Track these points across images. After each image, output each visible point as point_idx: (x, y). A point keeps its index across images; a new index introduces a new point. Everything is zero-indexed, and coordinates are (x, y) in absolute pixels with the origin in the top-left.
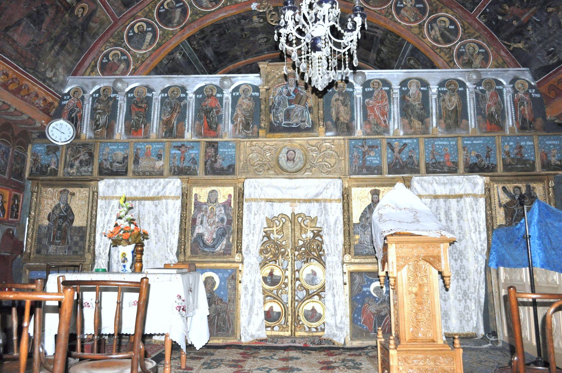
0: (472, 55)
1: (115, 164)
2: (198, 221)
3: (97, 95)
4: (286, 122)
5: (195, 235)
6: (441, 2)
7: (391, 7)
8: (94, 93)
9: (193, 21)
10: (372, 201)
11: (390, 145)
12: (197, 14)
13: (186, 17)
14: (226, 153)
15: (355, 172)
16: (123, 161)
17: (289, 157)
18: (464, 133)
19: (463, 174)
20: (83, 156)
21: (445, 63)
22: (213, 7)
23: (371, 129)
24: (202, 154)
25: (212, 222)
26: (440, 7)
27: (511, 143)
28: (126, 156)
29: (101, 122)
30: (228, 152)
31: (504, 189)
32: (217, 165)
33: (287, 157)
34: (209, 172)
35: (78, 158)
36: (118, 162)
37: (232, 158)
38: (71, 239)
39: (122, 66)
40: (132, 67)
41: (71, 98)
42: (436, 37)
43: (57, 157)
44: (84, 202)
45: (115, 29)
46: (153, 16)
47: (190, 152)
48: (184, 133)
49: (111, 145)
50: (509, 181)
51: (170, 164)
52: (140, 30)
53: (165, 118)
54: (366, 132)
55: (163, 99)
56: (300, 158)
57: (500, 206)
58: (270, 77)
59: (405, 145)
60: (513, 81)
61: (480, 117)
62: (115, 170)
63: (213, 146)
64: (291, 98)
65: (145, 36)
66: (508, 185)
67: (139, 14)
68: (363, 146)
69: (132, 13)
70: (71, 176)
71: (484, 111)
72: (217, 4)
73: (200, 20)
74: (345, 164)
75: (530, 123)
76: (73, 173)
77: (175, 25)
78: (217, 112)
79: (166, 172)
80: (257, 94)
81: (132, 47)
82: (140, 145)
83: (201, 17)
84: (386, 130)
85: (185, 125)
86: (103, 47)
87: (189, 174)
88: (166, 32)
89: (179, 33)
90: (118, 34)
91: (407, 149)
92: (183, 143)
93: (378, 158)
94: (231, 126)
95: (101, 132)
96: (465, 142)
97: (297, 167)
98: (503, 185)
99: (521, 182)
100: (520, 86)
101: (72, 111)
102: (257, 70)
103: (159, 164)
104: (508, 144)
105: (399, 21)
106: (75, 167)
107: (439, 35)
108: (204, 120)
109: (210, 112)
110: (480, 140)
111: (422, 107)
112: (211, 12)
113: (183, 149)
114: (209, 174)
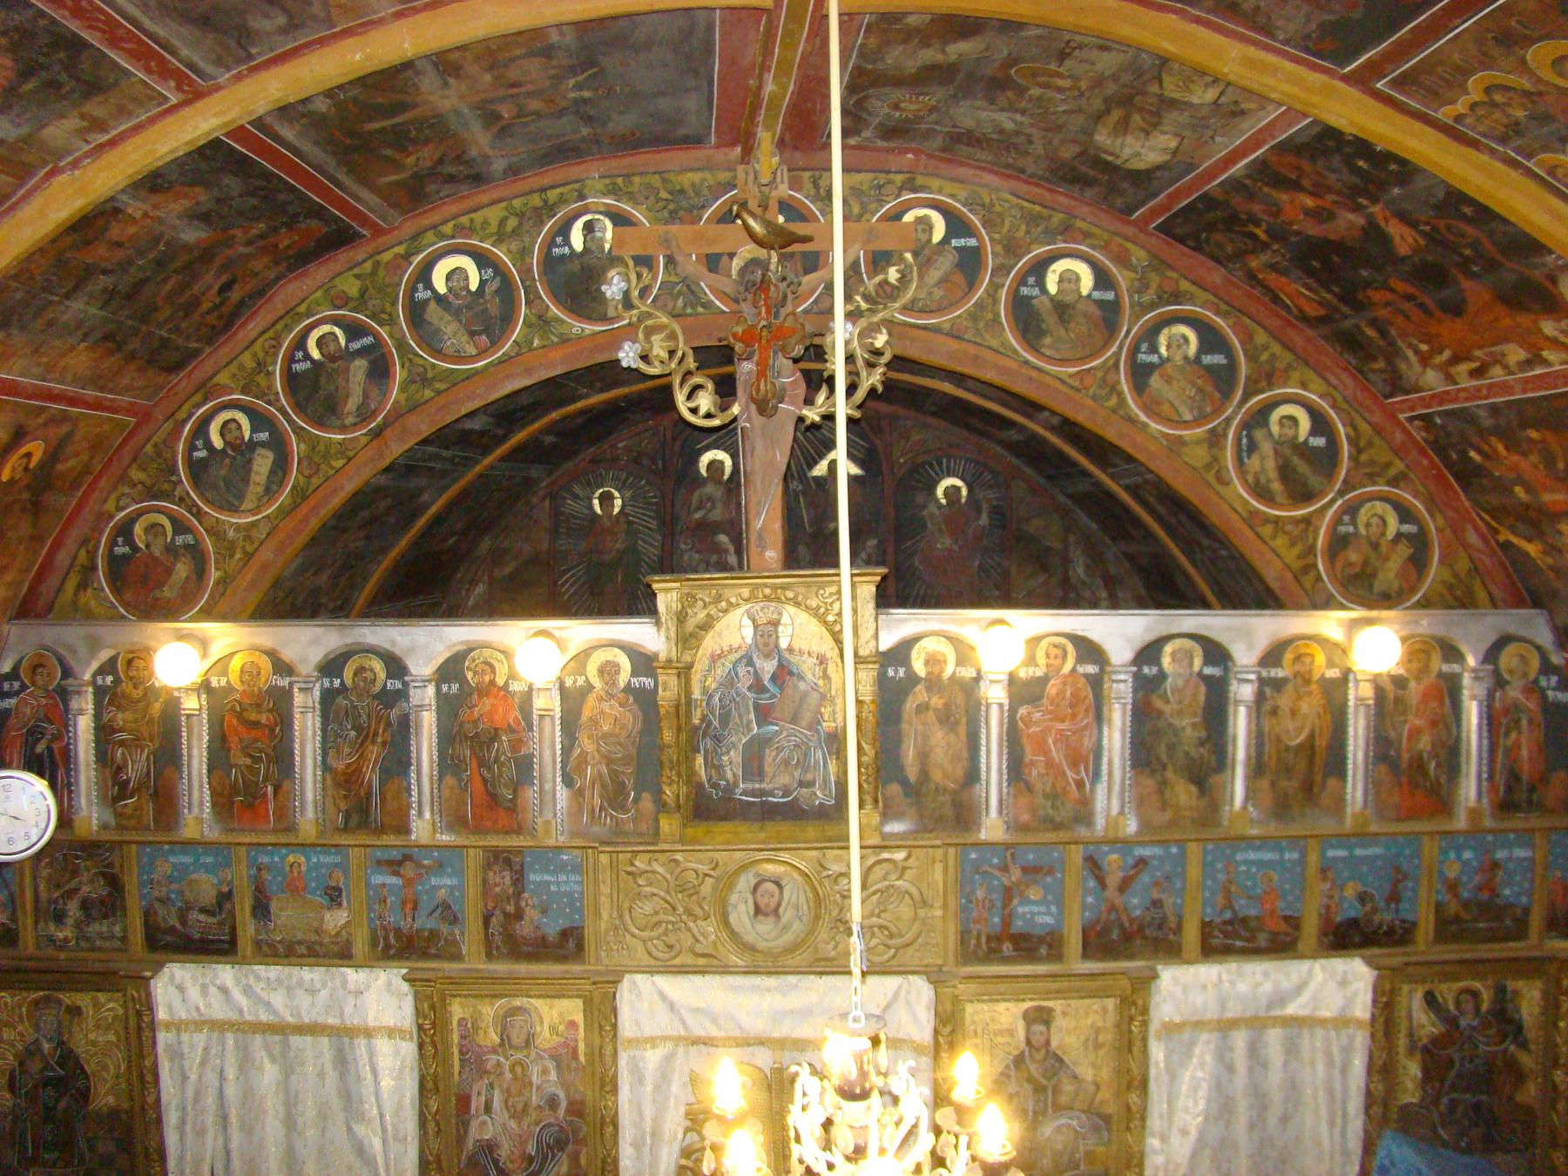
0: (1375, 546)
1: (194, 916)
2: (477, 1102)
3: (109, 679)
5: (470, 1144)
7: (1116, 365)
8: (94, 675)
9: (414, 407)
10: (1028, 1042)
11: (1093, 865)
12: (425, 381)
13: (385, 393)
15: (975, 952)
16: (220, 906)
17: (762, 902)
18: (1327, 825)
19: (1314, 957)
20: (92, 888)
21: (1289, 576)
22: (482, 353)
24: (473, 891)
25: (520, 1107)
26: (1280, 365)
27: (1467, 855)
28: (225, 889)
30: (558, 883)
31: (1430, 999)
32: (524, 929)
33: (756, 904)
34: (498, 948)
35: (76, 890)
36: (203, 910)
38: (92, 1148)
39: (182, 570)
40: (214, 575)
41: (24, 687)
42: (1263, 480)
44: (111, 1037)
47: (434, 881)
48: (408, 816)
49: (172, 852)
50: (1445, 977)
51: (371, 920)
52: (228, 438)
53: (340, 766)
54: (1016, 821)
55: (328, 697)
56: (797, 907)
57: (1411, 1050)
58: (691, 625)
59: (1142, 862)
60: (1491, 655)
61: (1383, 768)
62: (197, 936)
63: (508, 862)
65: (250, 461)
66: (1444, 987)
67: (223, 378)
68: (1004, 868)
69: (199, 375)
70: (61, 948)
71: (1398, 751)
72: (495, 342)
73: (442, 400)
74: (943, 929)
75: (1532, 789)
76: (66, 940)
77: (349, 420)
78: (516, 745)
79: (360, 947)
80: (648, 682)
81: (208, 502)
82: (267, 853)
83: (439, 393)
84: (1084, 814)
85: (409, 790)
86: (113, 497)
87: (437, 957)
88: (322, 447)
89: (370, 452)
90: (159, 454)
91: (1146, 878)
93: (1053, 909)
94: (562, 794)
95: (138, 807)
96: (1330, 853)
97: (788, 938)
98: (1427, 987)
99: (1477, 976)
100: (1515, 662)
101: (34, 734)
103: (336, 919)
104: (1459, 857)
105: (1143, 418)
106: (70, 921)
107: (1272, 473)
108: (471, 771)
110: (1377, 845)
111: (1203, 734)
112: (476, 372)
113: (408, 870)
114: (502, 957)
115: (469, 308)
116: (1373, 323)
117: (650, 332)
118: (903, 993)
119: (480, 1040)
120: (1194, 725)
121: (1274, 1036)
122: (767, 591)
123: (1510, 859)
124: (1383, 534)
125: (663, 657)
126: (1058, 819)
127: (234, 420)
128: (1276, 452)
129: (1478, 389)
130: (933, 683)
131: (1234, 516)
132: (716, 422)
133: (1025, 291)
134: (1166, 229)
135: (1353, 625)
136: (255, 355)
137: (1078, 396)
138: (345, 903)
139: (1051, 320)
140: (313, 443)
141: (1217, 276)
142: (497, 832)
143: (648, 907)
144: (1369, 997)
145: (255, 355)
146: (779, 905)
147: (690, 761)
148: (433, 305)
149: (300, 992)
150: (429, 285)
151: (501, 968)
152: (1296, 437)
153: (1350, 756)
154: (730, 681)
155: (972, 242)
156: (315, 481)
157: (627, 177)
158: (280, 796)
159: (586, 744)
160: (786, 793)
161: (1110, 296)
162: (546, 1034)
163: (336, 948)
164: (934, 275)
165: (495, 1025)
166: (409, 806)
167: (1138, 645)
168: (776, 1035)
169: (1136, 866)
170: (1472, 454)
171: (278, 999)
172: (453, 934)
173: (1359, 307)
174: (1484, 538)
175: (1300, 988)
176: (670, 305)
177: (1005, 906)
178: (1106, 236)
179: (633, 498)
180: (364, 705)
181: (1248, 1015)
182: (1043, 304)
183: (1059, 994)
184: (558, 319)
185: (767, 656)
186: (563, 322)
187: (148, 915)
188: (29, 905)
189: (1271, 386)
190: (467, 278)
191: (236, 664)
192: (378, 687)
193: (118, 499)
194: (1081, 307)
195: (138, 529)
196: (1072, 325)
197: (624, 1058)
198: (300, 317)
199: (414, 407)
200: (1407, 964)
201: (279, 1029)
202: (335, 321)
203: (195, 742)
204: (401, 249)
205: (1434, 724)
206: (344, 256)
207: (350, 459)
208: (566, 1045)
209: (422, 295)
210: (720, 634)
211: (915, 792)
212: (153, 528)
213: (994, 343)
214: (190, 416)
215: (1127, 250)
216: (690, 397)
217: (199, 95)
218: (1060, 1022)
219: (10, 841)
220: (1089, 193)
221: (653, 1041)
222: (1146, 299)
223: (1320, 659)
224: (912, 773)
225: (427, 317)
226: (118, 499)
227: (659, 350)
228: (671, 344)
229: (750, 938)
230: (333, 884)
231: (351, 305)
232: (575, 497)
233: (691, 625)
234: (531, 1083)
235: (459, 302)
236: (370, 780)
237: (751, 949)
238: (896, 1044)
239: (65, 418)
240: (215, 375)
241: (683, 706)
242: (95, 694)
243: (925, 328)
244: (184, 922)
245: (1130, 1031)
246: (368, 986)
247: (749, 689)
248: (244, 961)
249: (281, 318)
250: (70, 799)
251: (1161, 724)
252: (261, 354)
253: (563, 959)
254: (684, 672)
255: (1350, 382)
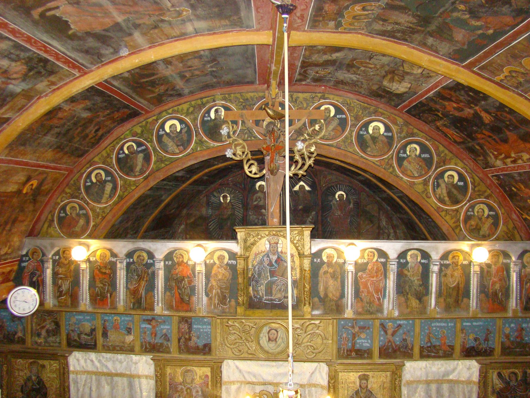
0: (480, 219)
1: (83, 336)
3: (57, 257)
4: (267, 297)
6: (450, 151)
7: (392, 158)
8: (53, 255)
9: (158, 170)
10: (360, 386)
13: (149, 164)
14: (201, 330)
15: (343, 355)
17: (271, 337)
18: (463, 314)
19: (459, 359)
22: (181, 152)
23: (363, 308)
24: (175, 331)
26: (448, 158)
27: (512, 325)
28: (93, 327)
29: (64, 288)
30: (203, 329)
31: (499, 375)
32: (191, 344)
33: (269, 337)
36: (86, 334)
37: (207, 336)
39: (82, 222)
40: (92, 224)
41: (30, 259)
42: (442, 197)
43: (23, 325)
45: (71, 176)
46: (112, 162)
47: (162, 327)
48: (154, 305)
49: (76, 315)
51: (141, 339)
52: (98, 179)
53: (132, 288)
54: (357, 311)
55: (128, 265)
57: (493, 392)
58: (248, 243)
59: (400, 326)
60: (521, 256)
61: (483, 295)
62: (84, 343)
64: (273, 269)
65: (105, 186)
66: (504, 371)
67: (96, 159)
68: (353, 327)
69: (88, 158)
71: (488, 289)
72: (185, 149)
73: (168, 167)
76: (41, 342)
77: (137, 174)
78: (190, 282)
79: (137, 348)
80: (234, 262)
81: (91, 200)
82: (107, 316)
83: (167, 165)
84: (380, 309)
85: (154, 296)
87: (162, 352)
88: (128, 182)
90: (75, 184)
92: (153, 316)
93: (369, 341)
94: (205, 299)
96: (464, 324)
98: (498, 370)
101: (33, 274)
102: (233, 237)
103: (129, 339)
105: (401, 175)
106: (42, 336)
107: (445, 195)
108: (175, 291)
109: (181, 283)
110: (480, 321)
111: (421, 283)
112: (178, 159)
113: (154, 323)
115: (177, 137)
116: (478, 144)
117: (236, 146)
118: (318, 368)
119: (176, 380)
120: (418, 280)
121: (445, 387)
122: (274, 232)
123: (528, 327)
124: (483, 215)
125: (239, 254)
126: (371, 310)
127: (100, 173)
128: (446, 187)
129: (514, 167)
130: (329, 264)
131: (431, 208)
132: (258, 176)
133: (361, 133)
134: (408, 112)
135: (473, 246)
136: (107, 152)
137: (379, 168)
138: (132, 333)
139: (370, 143)
140: (125, 181)
141: (426, 128)
142: (183, 311)
143: (233, 337)
144: (478, 374)
145: (107, 152)
146: (277, 338)
147: (247, 289)
148: (165, 136)
149: (117, 363)
150: (164, 130)
151: (183, 356)
152: (453, 182)
153: (471, 291)
154: (261, 262)
155: (344, 116)
156: (126, 194)
157: (229, 94)
158: (112, 298)
159: (213, 282)
160: (280, 300)
161: (390, 134)
162: (198, 379)
163: (129, 348)
164: (331, 127)
165: (181, 375)
166: (154, 302)
167: (399, 252)
168: (275, 381)
169: (398, 327)
170: (513, 188)
171: (110, 365)
172: (168, 345)
173: (473, 139)
174: (519, 217)
175: (454, 370)
176: (243, 137)
177: (353, 340)
178: (389, 114)
179: (233, 197)
180: (140, 268)
181: (436, 379)
182: (367, 137)
183: (371, 370)
184: (206, 141)
185: (274, 254)
186: (208, 142)
187: (68, 335)
188: (29, 332)
189: (445, 164)
190: (176, 127)
191: (98, 253)
192: (145, 262)
193: (62, 198)
194: (380, 138)
195: (68, 208)
196: (377, 144)
197: (224, 388)
198: (122, 140)
199: (158, 170)
200: (491, 363)
201: (110, 375)
202: (133, 141)
203: (85, 279)
204: (155, 118)
205: (500, 280)
206: (136, 120)
207: (137, 187)
208: (205, 383)
209: (161, 133)
210: (258, 246)
211: (323, 301)
212: (73, 208)
213: (351, 150)
214: (85, 171)
215: (396, 119)
216: (249, 167)
217: (86, 73)
218: (371, 379)
219: (24, 310)
220: (383, 100)
221: (233, 382)
222: (402, 135)
223: (461, 258)
224: (322, 294)
225: (163, 140)
226: (62, 198)
227: (239, 152)
228: (243, 150)
229: (267, 348)
230: (128, 327)
231: (139, 136)
232: (214, 196)
233: (248, 243)
234: (192, 395)
235: (173, 135)
236: (142, 293)
237: (268, 352)
238: (315, 385)
239: (44, 172)
240: (94, 158)
241: (245, 270)
242: (53, 262)
243: (328, 145)
244: (79, 338)
245: (395, 383)
246: (139, 361)
247: (268, 265)
248: (99, 352)
249: (115, 140)
250: (44, 296)
251: (407, 279)
252: (109, 152)
253: (204, 354)
254: (246, 259)
255: (472, 164)
